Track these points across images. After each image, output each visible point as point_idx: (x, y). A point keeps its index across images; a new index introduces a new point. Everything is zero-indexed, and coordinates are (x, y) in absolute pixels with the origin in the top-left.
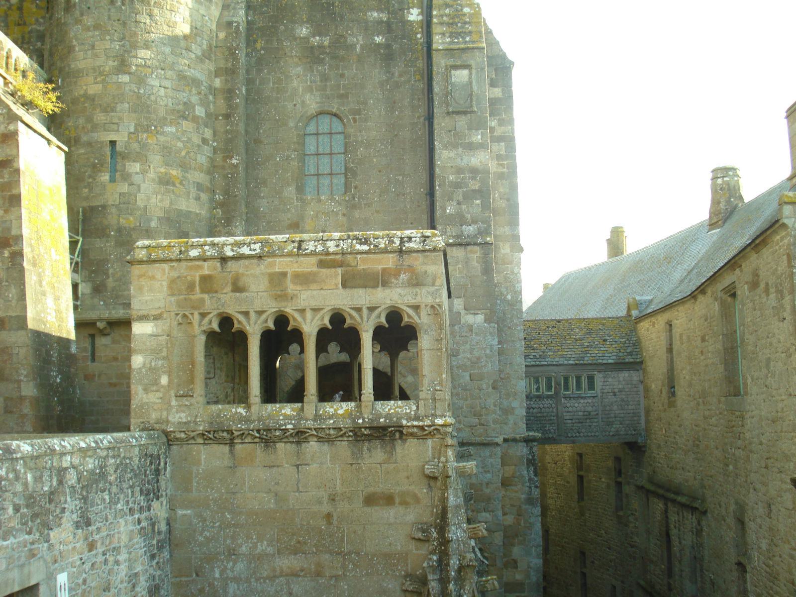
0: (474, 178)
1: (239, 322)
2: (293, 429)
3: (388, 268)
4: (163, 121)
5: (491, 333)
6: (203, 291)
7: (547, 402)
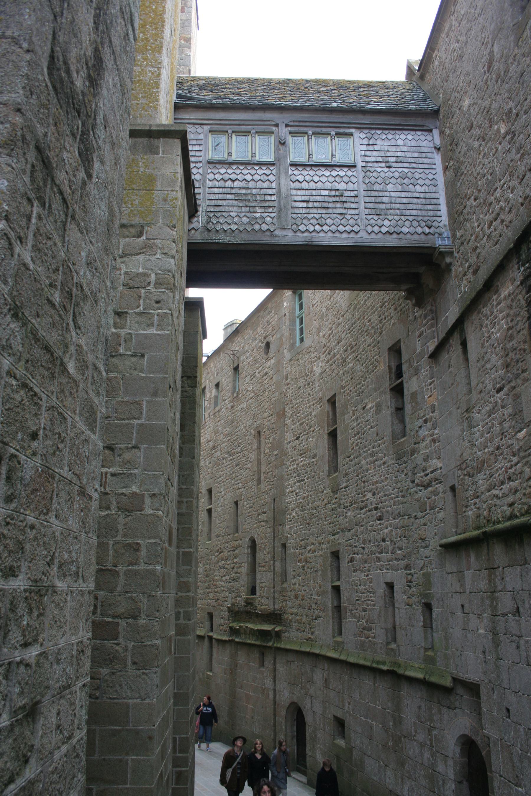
7: (260, 172)
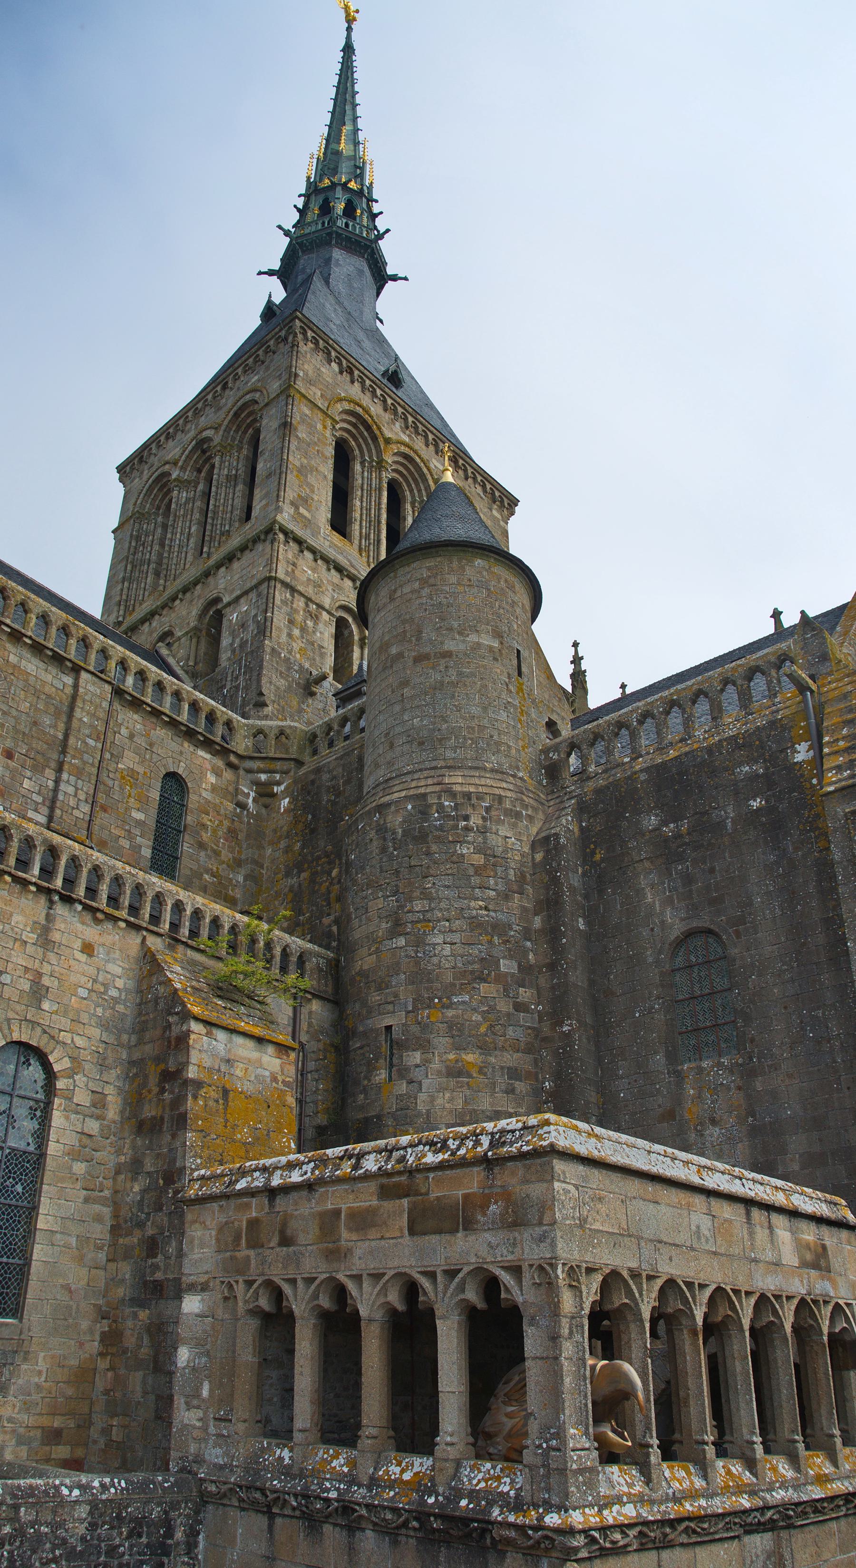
3: (473, 1193)
4: (450, 990)
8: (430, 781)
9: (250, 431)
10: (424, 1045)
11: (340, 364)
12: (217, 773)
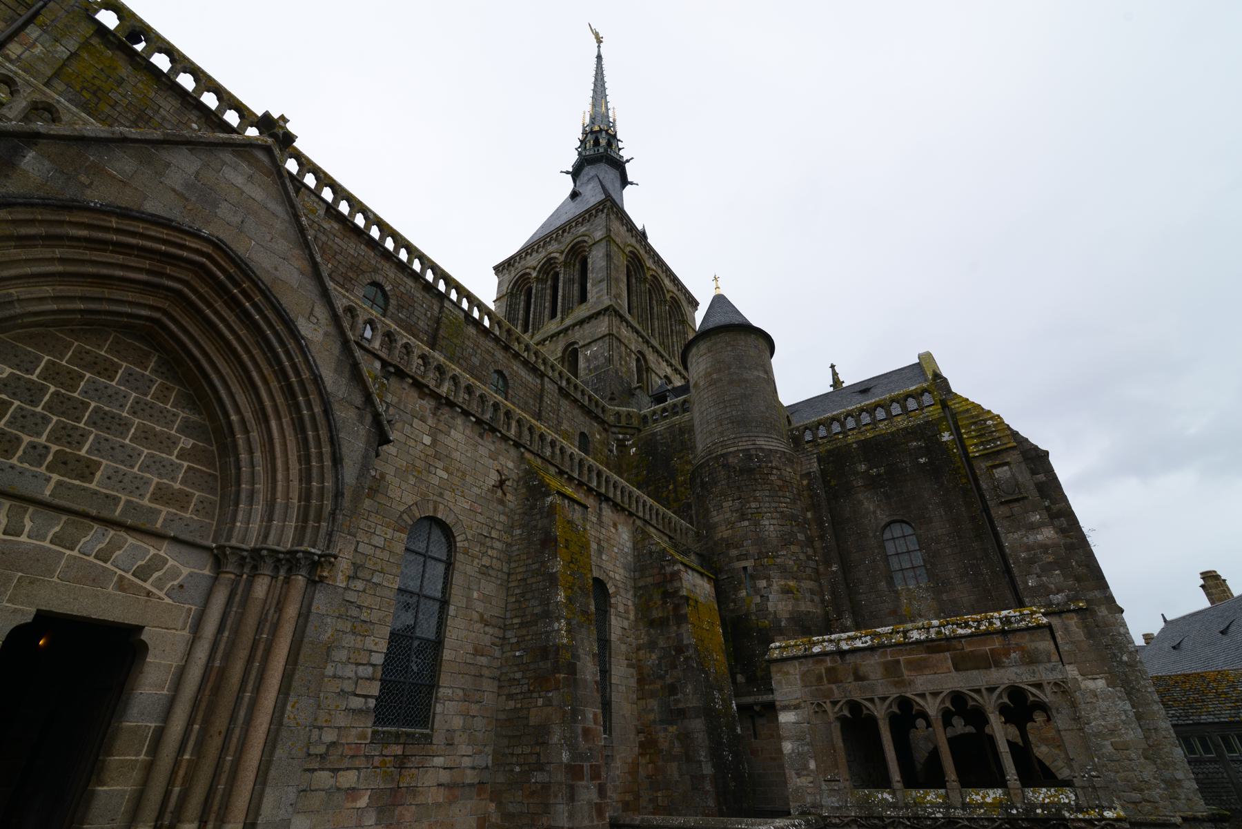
0: (1046, 552)
1: (868, 709)
2: (942, 818)
5: (1119, 698)
6: (829, 682)
8: (749, 443)
9: (580, 257)
10: (768, 578)
11: (627, 226)
12: (600, 435)
